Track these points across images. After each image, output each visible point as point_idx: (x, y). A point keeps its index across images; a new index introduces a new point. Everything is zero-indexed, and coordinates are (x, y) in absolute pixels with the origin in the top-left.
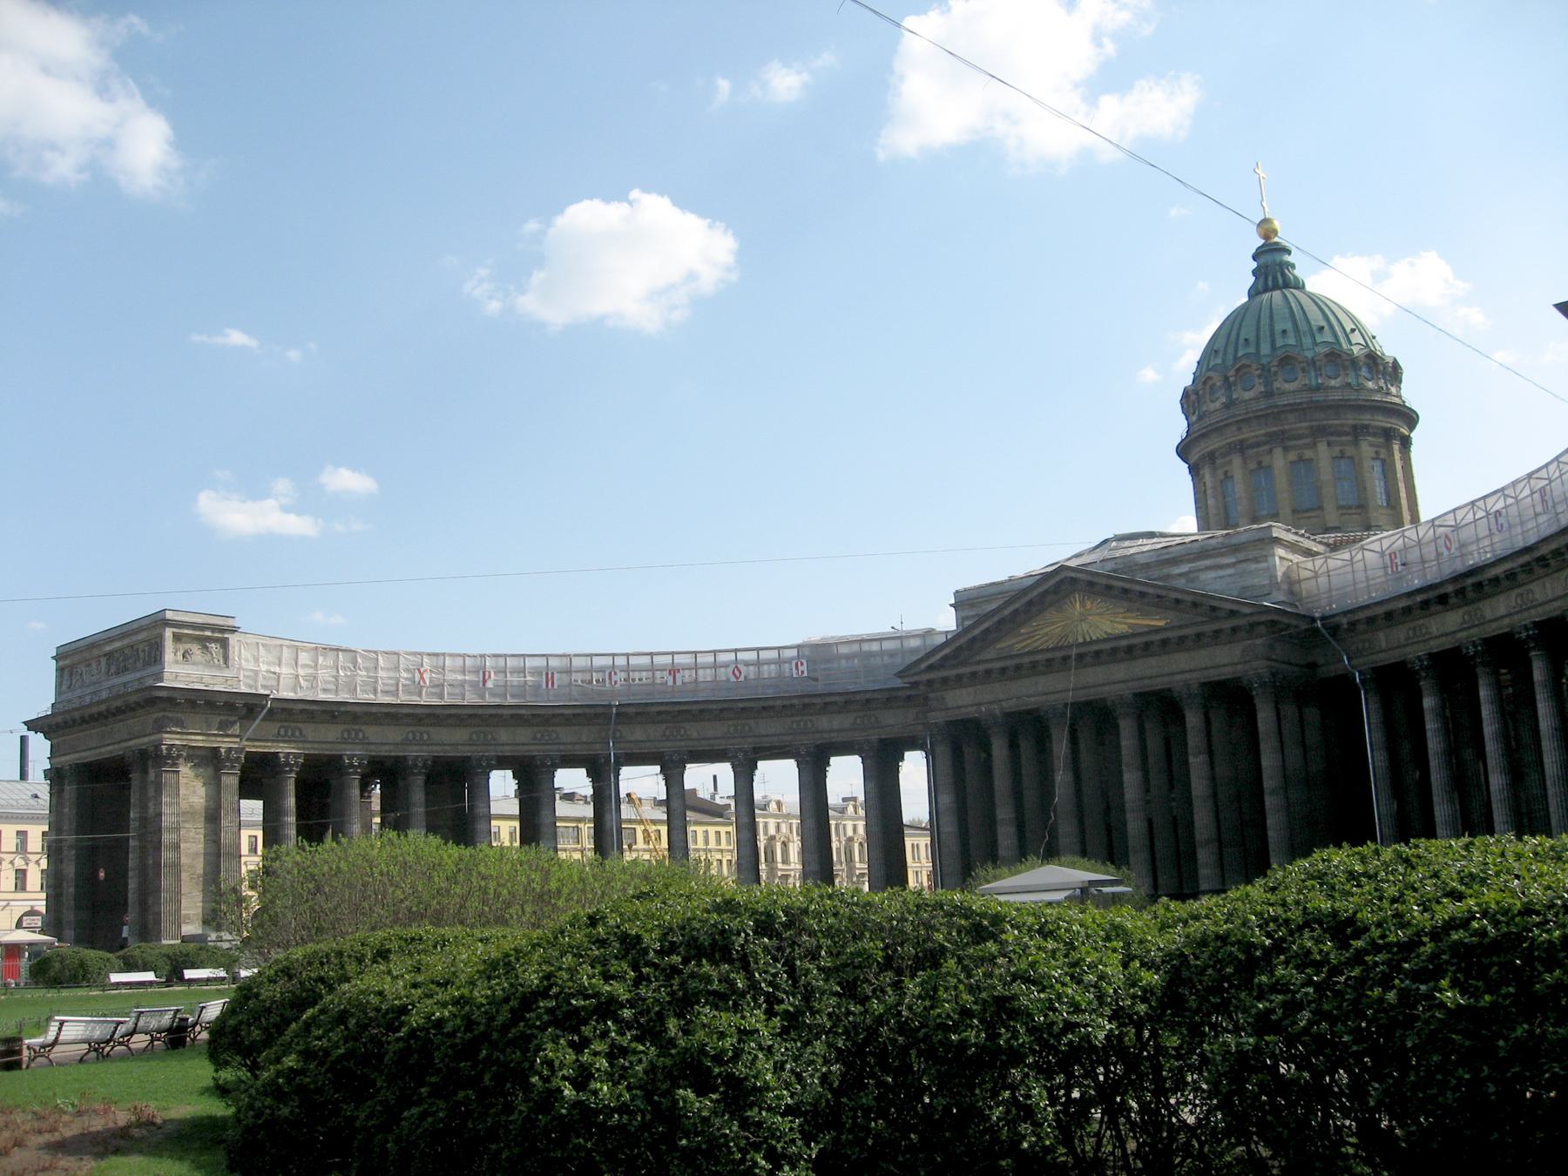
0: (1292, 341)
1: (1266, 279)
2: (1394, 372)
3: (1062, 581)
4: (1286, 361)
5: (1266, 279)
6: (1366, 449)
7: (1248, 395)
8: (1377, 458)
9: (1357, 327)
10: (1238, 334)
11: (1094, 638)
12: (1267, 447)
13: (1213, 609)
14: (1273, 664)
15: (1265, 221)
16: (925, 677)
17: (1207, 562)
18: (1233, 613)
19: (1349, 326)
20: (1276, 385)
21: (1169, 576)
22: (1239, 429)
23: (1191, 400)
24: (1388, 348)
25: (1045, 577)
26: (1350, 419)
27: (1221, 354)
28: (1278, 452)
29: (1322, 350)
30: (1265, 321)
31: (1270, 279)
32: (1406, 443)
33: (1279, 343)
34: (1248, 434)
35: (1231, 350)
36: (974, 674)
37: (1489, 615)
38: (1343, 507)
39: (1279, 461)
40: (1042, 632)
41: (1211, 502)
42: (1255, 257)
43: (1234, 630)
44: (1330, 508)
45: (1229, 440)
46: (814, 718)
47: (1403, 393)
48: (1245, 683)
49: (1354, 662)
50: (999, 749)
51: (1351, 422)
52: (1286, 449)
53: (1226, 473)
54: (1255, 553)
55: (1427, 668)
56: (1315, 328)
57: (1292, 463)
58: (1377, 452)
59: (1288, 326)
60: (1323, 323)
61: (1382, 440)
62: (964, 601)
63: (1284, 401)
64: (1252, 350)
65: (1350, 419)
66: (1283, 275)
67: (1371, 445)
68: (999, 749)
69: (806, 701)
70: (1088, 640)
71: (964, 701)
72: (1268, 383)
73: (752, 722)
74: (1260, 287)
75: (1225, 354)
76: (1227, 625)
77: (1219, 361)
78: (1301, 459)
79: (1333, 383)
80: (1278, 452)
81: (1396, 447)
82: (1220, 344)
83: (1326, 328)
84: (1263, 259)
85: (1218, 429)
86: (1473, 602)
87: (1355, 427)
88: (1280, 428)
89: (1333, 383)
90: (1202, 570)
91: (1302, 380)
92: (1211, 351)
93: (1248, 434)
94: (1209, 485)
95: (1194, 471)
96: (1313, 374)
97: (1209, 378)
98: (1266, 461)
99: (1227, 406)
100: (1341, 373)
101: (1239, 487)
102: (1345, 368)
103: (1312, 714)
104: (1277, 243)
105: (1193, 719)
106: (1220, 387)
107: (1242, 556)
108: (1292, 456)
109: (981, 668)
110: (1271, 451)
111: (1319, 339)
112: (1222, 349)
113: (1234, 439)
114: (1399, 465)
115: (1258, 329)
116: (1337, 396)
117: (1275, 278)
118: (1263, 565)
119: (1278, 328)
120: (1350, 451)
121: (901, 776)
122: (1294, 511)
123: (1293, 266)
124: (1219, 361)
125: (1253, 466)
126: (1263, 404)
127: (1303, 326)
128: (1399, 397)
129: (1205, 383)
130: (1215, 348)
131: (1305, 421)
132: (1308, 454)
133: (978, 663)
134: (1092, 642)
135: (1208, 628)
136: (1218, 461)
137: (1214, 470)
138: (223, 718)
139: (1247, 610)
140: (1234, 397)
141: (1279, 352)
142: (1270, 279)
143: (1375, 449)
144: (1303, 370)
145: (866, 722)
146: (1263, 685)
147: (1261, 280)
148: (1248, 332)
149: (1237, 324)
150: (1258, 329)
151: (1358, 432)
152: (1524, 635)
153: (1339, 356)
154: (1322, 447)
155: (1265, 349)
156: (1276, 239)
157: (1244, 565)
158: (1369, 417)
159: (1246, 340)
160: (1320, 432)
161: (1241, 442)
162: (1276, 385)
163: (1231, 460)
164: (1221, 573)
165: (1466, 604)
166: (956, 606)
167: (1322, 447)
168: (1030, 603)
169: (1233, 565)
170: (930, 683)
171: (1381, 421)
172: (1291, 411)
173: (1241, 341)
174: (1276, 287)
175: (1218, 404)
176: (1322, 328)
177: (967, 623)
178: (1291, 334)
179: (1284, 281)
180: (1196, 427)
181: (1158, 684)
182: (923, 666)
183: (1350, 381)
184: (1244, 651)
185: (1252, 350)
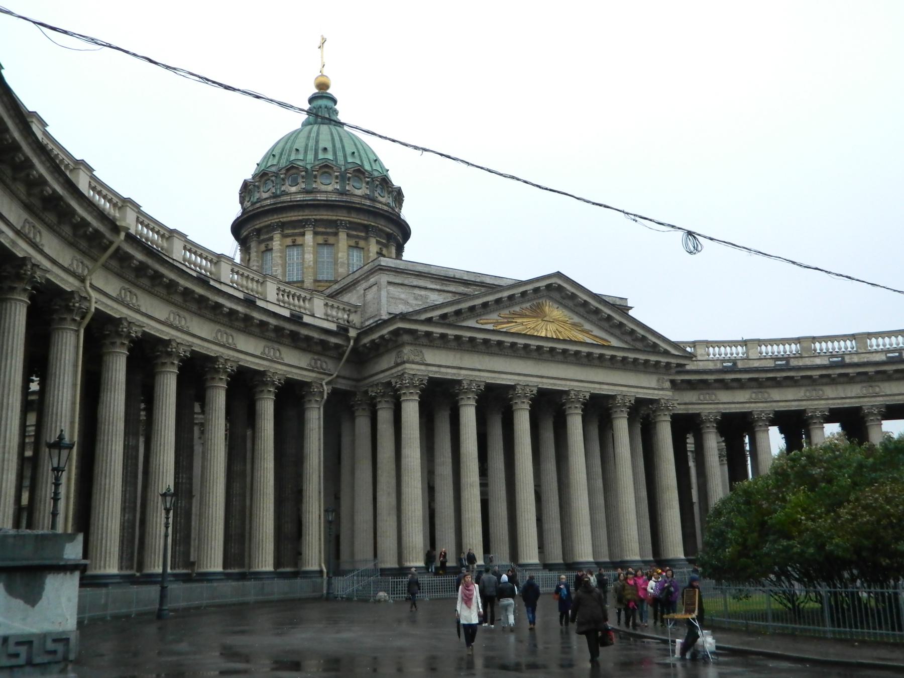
3: (549, 287)
7: (358, 192)
12: (363, 234)
13: (655, 345)
15: (322, 75)
18: (666, 353)
20: (376, 195)
28: (373, 241)
36: (458, 338)
40: (519, 320)
45: (339, 218)
46: (235, 335)
52: (378, 242)
63: (379, 206)
64: (301, 157)
70: (555, 337)
72: (373, 191)
76: (664, 360)
80: (373, 241)
85: (329, 206)
88: (376, 225)
97: (326, 166)
99: (336, 192)
106: (337, 177)
110: (366, 239)
113: (345, 219)
125: (352, 243)
126: (368, 203)
130: (322, 145)
131: (389, 229)
135: (653, 358)
137: (316, 234)
139: (677, 353)
140: (347, 188)
145: (272, 354)
152: (818, 414)
155: (367, 167)
156: (328, 91)
159: (353, 153)
161: (350, 222)
163: (336, 234)
175: (330, 188)
181: (606, 390)
182: (423, 317)
184: (658, 381)
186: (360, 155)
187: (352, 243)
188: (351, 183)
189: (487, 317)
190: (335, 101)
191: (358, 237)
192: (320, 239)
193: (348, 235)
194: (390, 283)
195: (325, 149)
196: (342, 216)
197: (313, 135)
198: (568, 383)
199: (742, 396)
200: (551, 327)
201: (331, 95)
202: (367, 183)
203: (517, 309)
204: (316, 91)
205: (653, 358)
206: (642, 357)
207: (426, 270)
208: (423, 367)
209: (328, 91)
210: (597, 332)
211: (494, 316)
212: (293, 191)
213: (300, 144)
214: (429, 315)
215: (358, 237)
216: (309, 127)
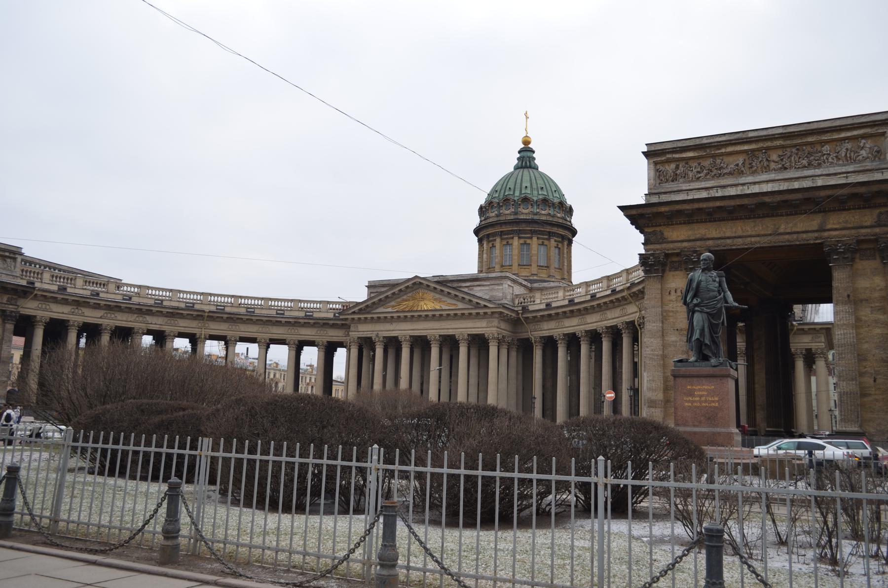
0: (528, 191)
1: (522, 163)
2: (570, 211)
3: (414, 284)
4: (526, 200)
5: (522, 163)
6: (553, 242)
7: (508, 212)
8: (557, 247)
9: (558, 190)
10: (507, 185)
11: (426, 309)
12: (512, 236)
13: (477, 303)
14: (499, 330)
15: (527, 136)
16: (350, 317)
17: (478, 283)
18: (485, 306)
19: (554, 189)
20: (520, 210)
21: (461, 287)
22: (501, 226)
23: (482, 210)
24: (569, 201)
25: (409, 280)
26: (548, 229)
27: (498, 193)
28: (516, 238)
29: (541, 197)
30: (519, 181)
31: (524, 163)
32: (570, 242)
33: (523, 192)
34: (504, 229)
35: (503, 191)
37: (589, 321)
38: (540, 266)
39: (516, 242)
41: (485, 256)
42: (519, 152)
43: (485, 313)
44: (534, 265)
46: (298, 328)
47: (573, 221)
48: (486, 336)
49: (532, 333)
50: (379, 352)
51: (548, 230)
52: (519, 238)
53: (493, 244)
54: (498, 282)
55: (563, 339)
56: (539, 187)
57: (521, 244)
58: (557, 245)
59: (528, 185)
60: (544, 186)
61: (560, 240)
62: (371, 286)
63: (522, 217)
64: (512, 193)
65: (548, 229)
66: (530, 162)
67: (555, 241)
68: (379, 352)
69: (296, 320)
71: (365, 330)
73: (270, 327)
74: (520, 165)
75: (500, 193)
76: (481, 311)
77: (497, 195)
78: (525, 243)
79: (543, 212)
80: (516, 238)
81: (566, 243)
82: (498, 188)
83: (544, 188)
84: (522, 154)
85: (491, 225)
86: (584, 315)
87: (549, 232)
89: (543, 212)
90: (474, 286)
91: (530, 209)
92: (494, 190)
93: (505, 228)
94: (485, 248)
95: (480, 241)
96: (535, 207)
97: (492, 202)
98: (510, 241)
99: (497, 216)
100: (548, 208)
101: (497, 251)
102: (550, 207)
103: (514, 354)
104: (530, 148)
105: (463, 350)
107: (493, 282)
108: (522, 241)
109: (375, 316)
110: (513, 238)
111: (540, 193)
112: (499, 190)
114: (565, 251)
115: (515, 185)
116: (544, 218)
117: (526, 163)
118: (501, 287)
119: (524, 185)
120: (546, 242)
121: (335, 359)
122: (519, 265)
123: (534, 159)
124: (497, 195)
126: (512, 217)
127: (535, 186)
128: (570, 222)
129: (489, 204)
132: (528, 241)
133: (374, 313)
134: (425, 311)
135: (474, 312)
136: (491, 239)
137: (489, 242)
138: (10, 296)
141: (523, 196)
142: (524, 163)
143: (556, 243)
144: (532, 205)
146: (494, 338)
147: (520, 163)
148: (511, 185)
149: (507, 179)
150: (515, 185)
151: (551, 234)
153: (548, 201)
154: (535, 239)
155: (517, 193)
156: (530, 146)
157: (493, 286)
158: (556, 229)
160: (533, 232)
161: (501, 232)
162: (520, 210)
163: (495, 240)
164: (483, 288)
165: (581, 315)
166: (368, 287)
167: (535, 239)
168: (400, 290)
169: (489, 285)
170: (353, 319)
171: (561, 231)
172: (524, 222)
173: (508, 188)
174: (527, 168)
175: (493, 214)
176: (542, 188)
177: (372, 295)
178: (529, 188)
179: (530, 164)
180: (483, 223)
181: (451, 332)
182: (350, 312)
183: (550, 212)
185: (512, 193)
186: (515, 188)
187: (505, 242)
188: (504, 208)
189: (389, 304)
190: (534, 152)
191: (507, 238)
192: (490, 245)
193: (502, 239)
194: (371, 293)
195: (496, 191)
196: (498, 229)
197: (520, 177)
198: (428, 331)
199: (575, 321)
200: (422, 303)
201: (532, 149)
202: (513, 205)
203: (405, 297)
204: (523, 146)
205: (474, 312)
206: (466, 312)
207: (388, 283)
208: (356, 333)
209: (530, 146)
210: (449, 301)
211: (393, 303)
212: (508, 213)
213: (511, 185)
214: (353, 310)
215: (507, 238)
216: (518, 170)
